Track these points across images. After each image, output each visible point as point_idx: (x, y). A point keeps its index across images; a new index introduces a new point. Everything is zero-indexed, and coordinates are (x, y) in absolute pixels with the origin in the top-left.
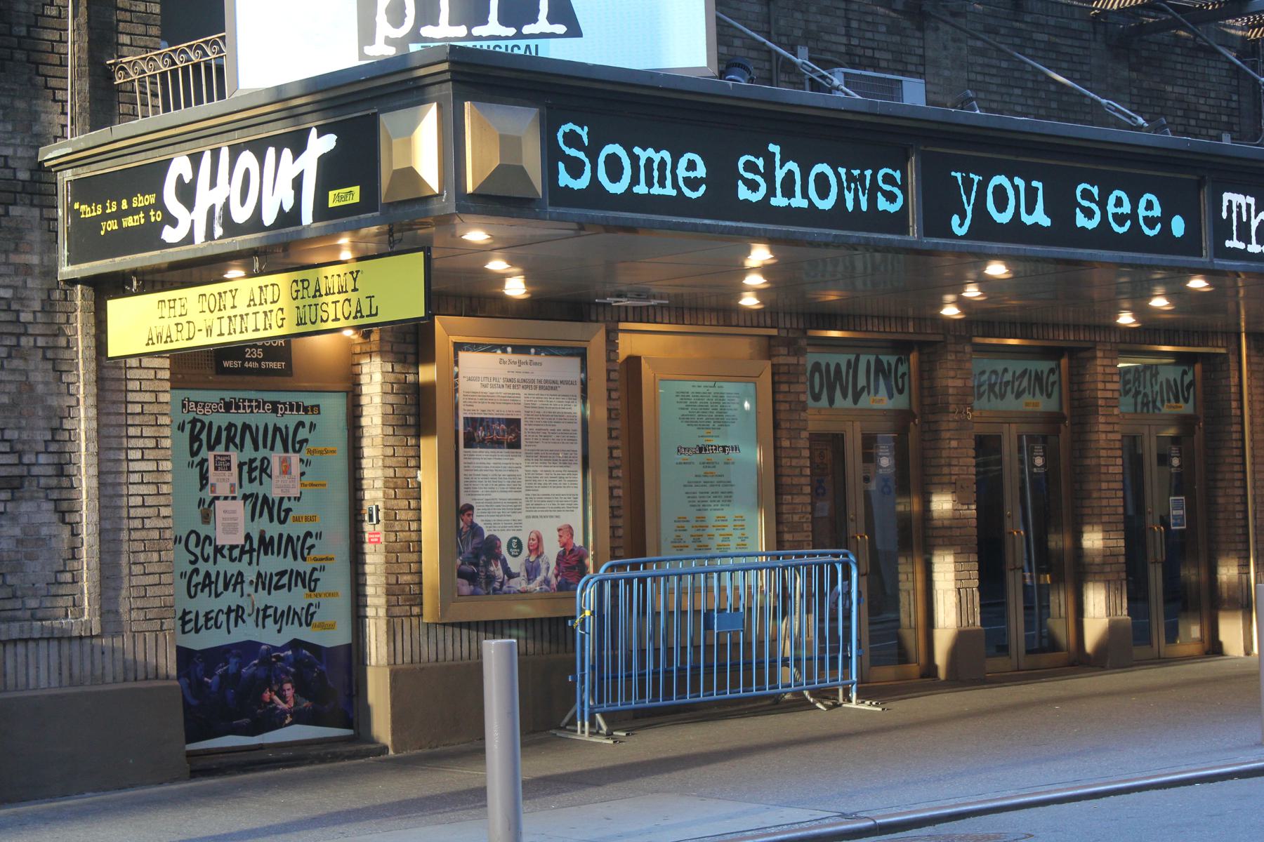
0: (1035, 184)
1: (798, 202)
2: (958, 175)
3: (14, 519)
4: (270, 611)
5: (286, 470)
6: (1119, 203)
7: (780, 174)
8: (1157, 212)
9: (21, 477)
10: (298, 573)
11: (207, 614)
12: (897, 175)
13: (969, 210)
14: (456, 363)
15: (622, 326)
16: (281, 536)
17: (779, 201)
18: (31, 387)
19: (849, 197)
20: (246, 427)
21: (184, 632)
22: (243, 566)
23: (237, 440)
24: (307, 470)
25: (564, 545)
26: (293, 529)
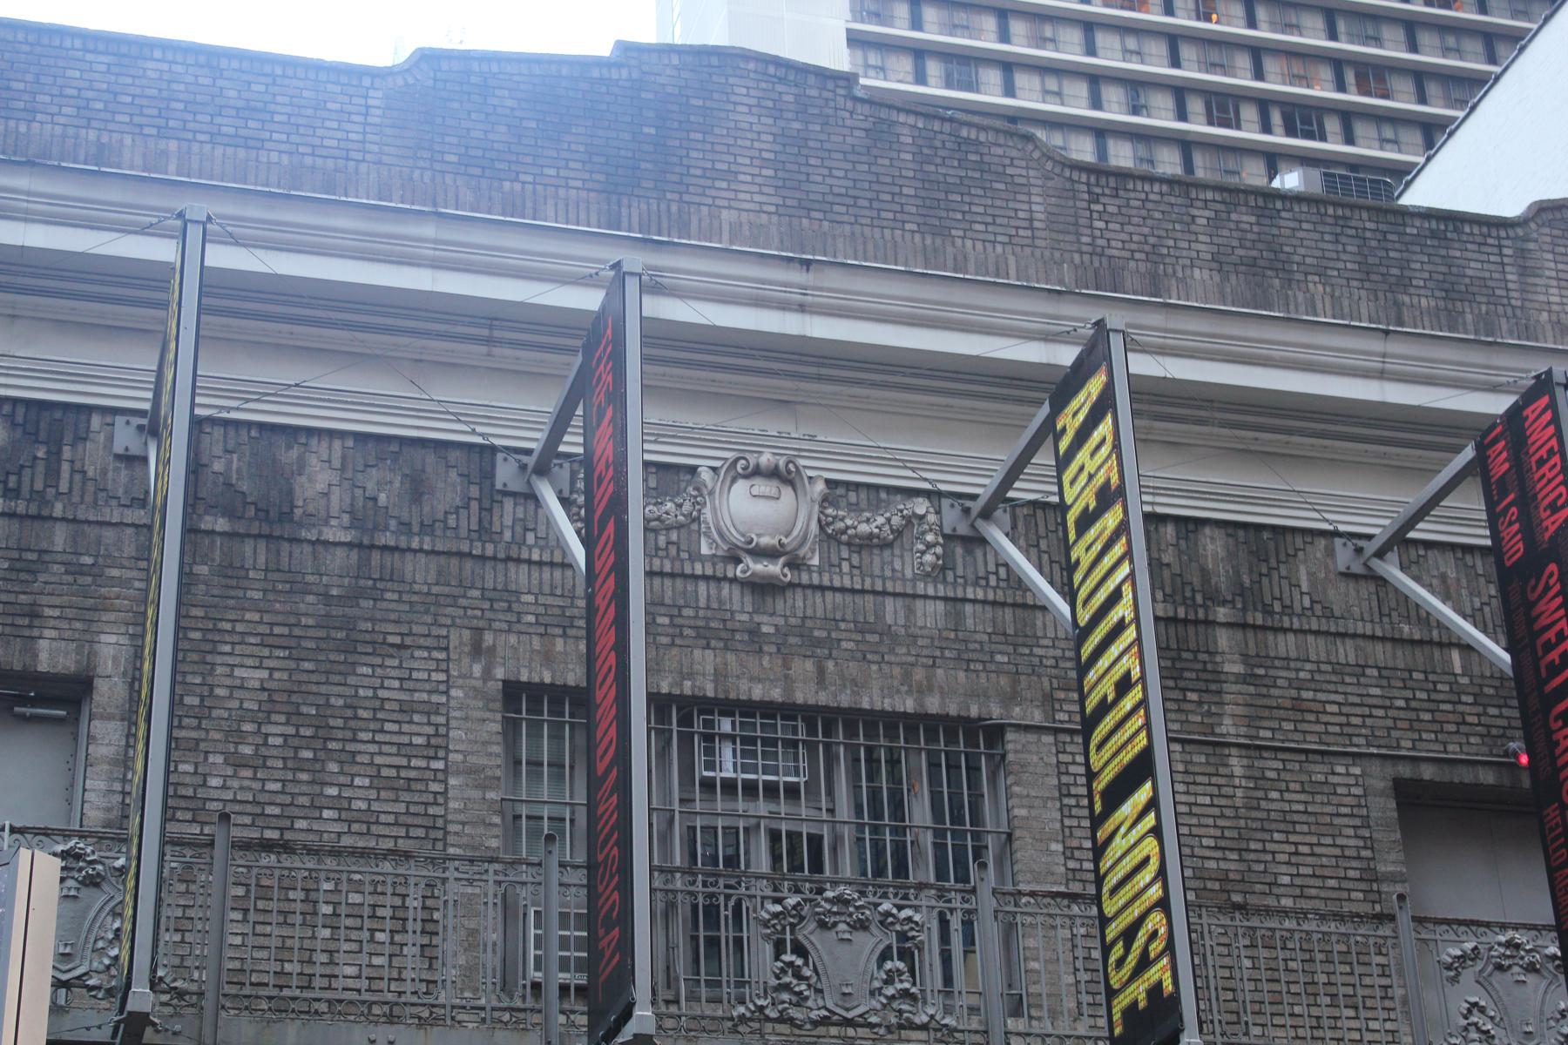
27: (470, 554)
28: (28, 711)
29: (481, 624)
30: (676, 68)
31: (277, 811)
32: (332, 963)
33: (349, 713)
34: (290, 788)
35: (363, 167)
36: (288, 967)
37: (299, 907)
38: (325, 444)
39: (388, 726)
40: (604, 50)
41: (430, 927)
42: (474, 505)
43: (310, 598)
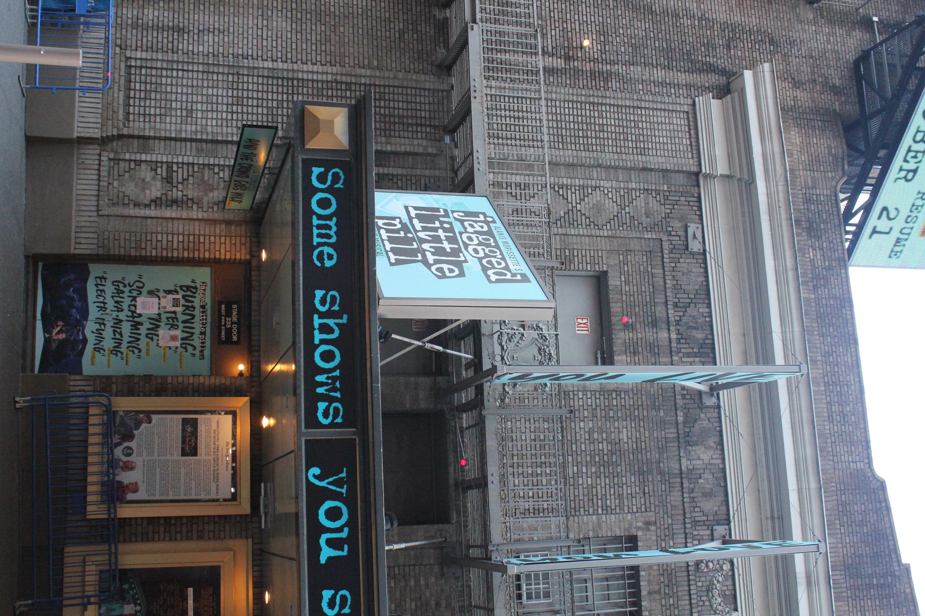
1: (318, 336)
2: (344, 475)
3: (154, 178)
4: (103, 327)
5: (174, 338)
7: (331, 322)
10: (120, 344)
12: (339, 420)
14: (226, 413)
15: (250, 540)
16: (140, 334)
17: (317, 321)
18: (212, 190)
20: (193, 316)
22: (126, 312)
23: (187, 312)
24: (172, 351)
25: (127, 486)
26: (142, 344)
27: (685, 518)
28: (599, 356)
29: (658, 525)
30: (904, 592)
31: (574, 449)
32: (519, 474)
33: (615, 474)
34: (583, 453)
35: (832, 463)
36: (515, 458)
37: (539, 460)
38: (718, 456)
39: (612, 490)
40: (905, 560)
41: (537, 512)
42: (705, 518)
43: (657, 455)
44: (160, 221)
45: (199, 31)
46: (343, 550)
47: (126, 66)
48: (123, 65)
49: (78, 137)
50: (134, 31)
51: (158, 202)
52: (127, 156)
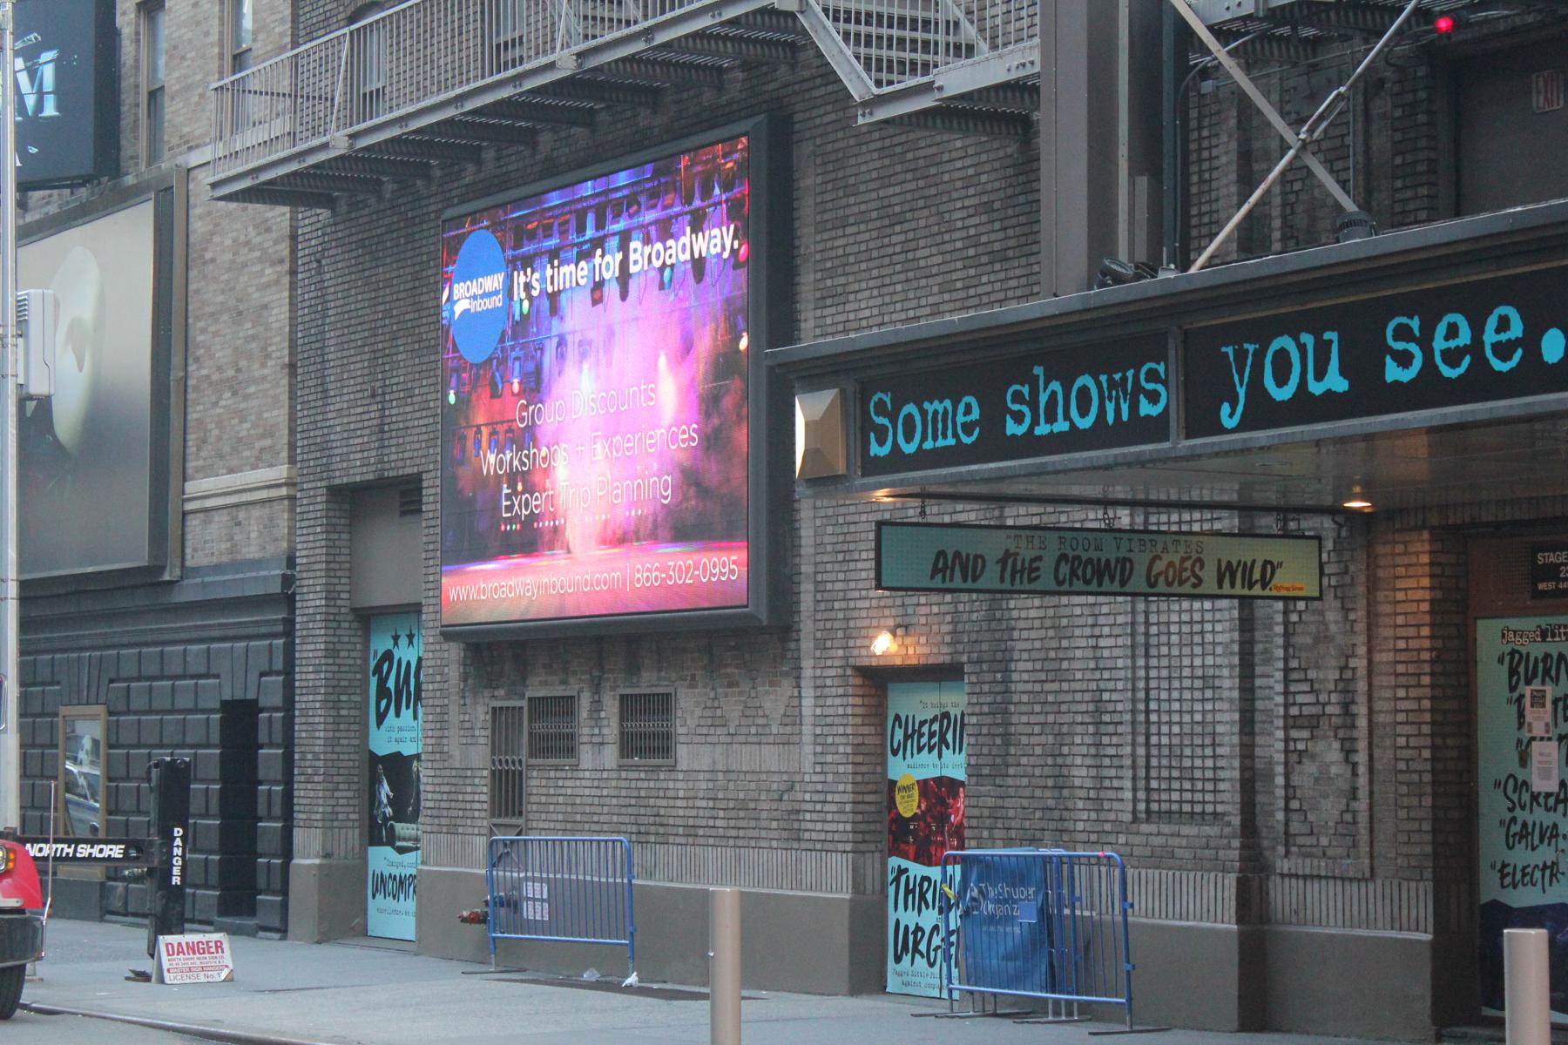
0: (1328, 336)
1: (1061, 426)
3: (1313, 757)
6: (1452, 332)
7: (1043, 398)
8: (1516, 330)
9: (1318, 716)
11: (1524, 868)
13: (1241, 392)
17: (1042, 429)
19: (1110, 408)
21: (1503, 886)
23: (1553, 673)
44: (1376, 740)
45: (1097, 669)
46: (1331, 342)
47: (1148, 821)
48: (1144, 828)
49: (1239, 921)
50: (1106, 805)
51: (1347, 745)
52: (1280, 816)
